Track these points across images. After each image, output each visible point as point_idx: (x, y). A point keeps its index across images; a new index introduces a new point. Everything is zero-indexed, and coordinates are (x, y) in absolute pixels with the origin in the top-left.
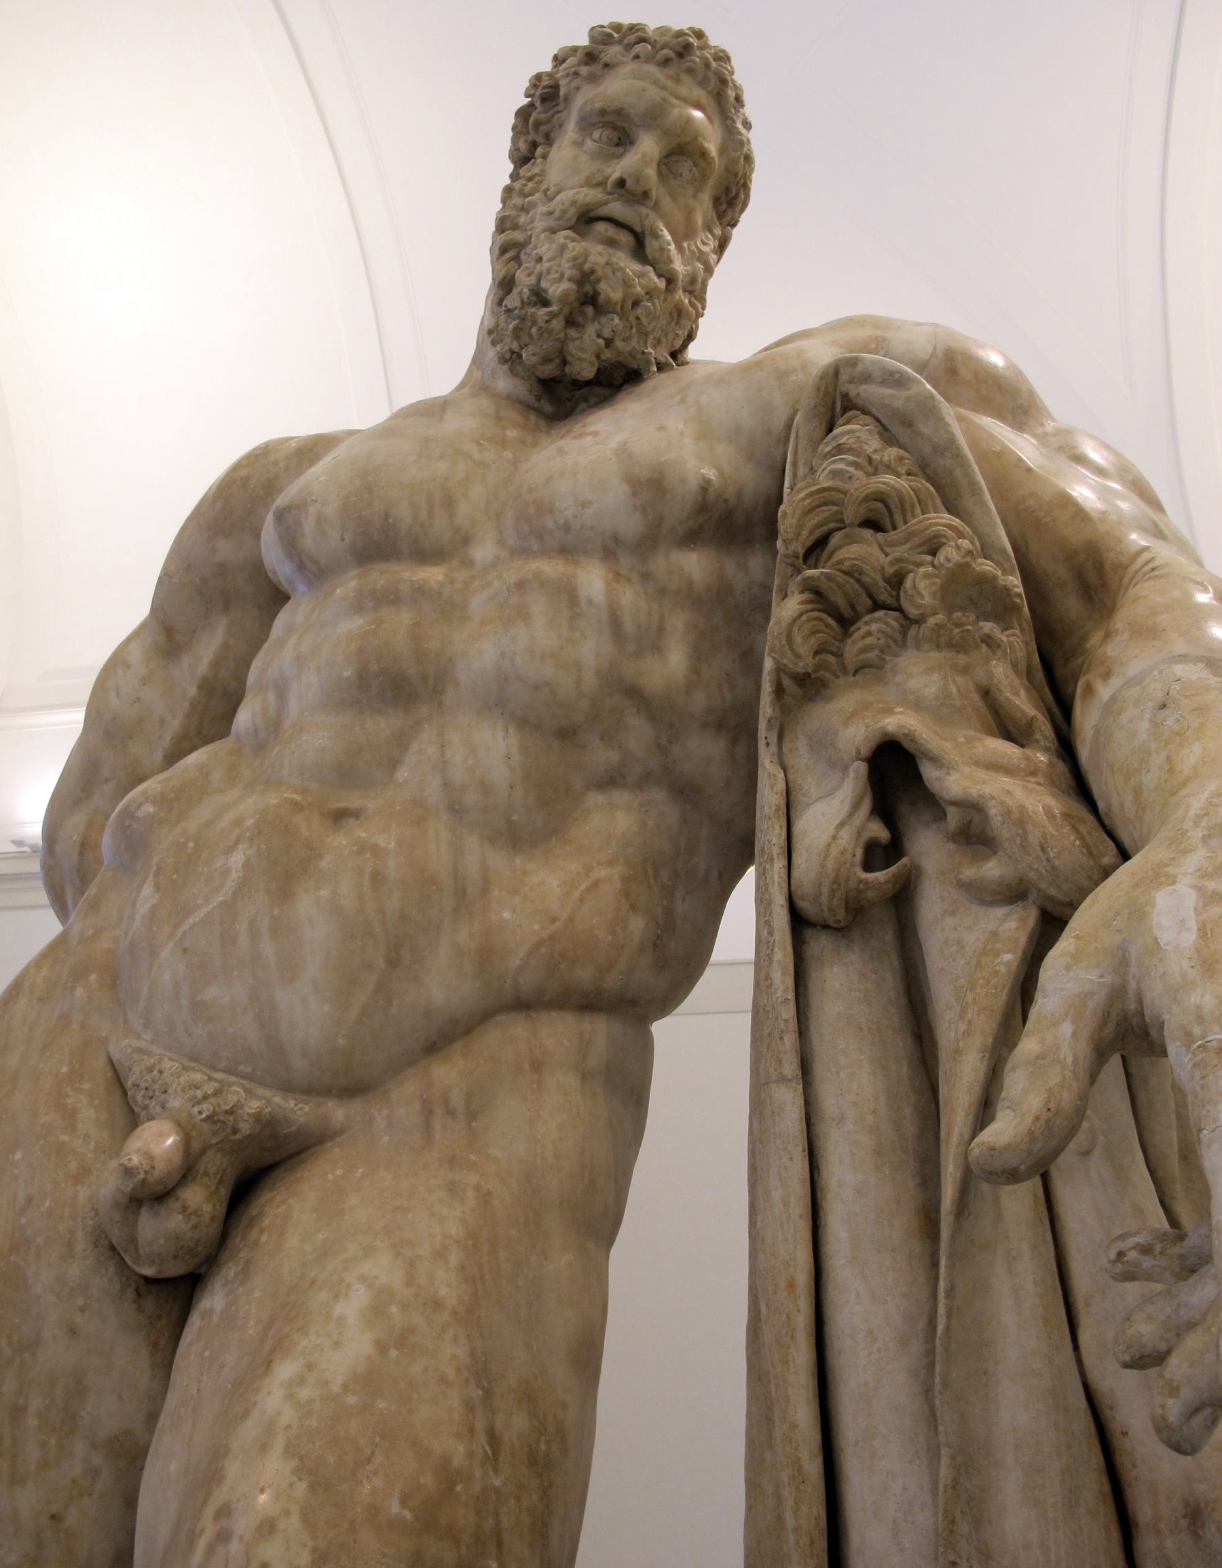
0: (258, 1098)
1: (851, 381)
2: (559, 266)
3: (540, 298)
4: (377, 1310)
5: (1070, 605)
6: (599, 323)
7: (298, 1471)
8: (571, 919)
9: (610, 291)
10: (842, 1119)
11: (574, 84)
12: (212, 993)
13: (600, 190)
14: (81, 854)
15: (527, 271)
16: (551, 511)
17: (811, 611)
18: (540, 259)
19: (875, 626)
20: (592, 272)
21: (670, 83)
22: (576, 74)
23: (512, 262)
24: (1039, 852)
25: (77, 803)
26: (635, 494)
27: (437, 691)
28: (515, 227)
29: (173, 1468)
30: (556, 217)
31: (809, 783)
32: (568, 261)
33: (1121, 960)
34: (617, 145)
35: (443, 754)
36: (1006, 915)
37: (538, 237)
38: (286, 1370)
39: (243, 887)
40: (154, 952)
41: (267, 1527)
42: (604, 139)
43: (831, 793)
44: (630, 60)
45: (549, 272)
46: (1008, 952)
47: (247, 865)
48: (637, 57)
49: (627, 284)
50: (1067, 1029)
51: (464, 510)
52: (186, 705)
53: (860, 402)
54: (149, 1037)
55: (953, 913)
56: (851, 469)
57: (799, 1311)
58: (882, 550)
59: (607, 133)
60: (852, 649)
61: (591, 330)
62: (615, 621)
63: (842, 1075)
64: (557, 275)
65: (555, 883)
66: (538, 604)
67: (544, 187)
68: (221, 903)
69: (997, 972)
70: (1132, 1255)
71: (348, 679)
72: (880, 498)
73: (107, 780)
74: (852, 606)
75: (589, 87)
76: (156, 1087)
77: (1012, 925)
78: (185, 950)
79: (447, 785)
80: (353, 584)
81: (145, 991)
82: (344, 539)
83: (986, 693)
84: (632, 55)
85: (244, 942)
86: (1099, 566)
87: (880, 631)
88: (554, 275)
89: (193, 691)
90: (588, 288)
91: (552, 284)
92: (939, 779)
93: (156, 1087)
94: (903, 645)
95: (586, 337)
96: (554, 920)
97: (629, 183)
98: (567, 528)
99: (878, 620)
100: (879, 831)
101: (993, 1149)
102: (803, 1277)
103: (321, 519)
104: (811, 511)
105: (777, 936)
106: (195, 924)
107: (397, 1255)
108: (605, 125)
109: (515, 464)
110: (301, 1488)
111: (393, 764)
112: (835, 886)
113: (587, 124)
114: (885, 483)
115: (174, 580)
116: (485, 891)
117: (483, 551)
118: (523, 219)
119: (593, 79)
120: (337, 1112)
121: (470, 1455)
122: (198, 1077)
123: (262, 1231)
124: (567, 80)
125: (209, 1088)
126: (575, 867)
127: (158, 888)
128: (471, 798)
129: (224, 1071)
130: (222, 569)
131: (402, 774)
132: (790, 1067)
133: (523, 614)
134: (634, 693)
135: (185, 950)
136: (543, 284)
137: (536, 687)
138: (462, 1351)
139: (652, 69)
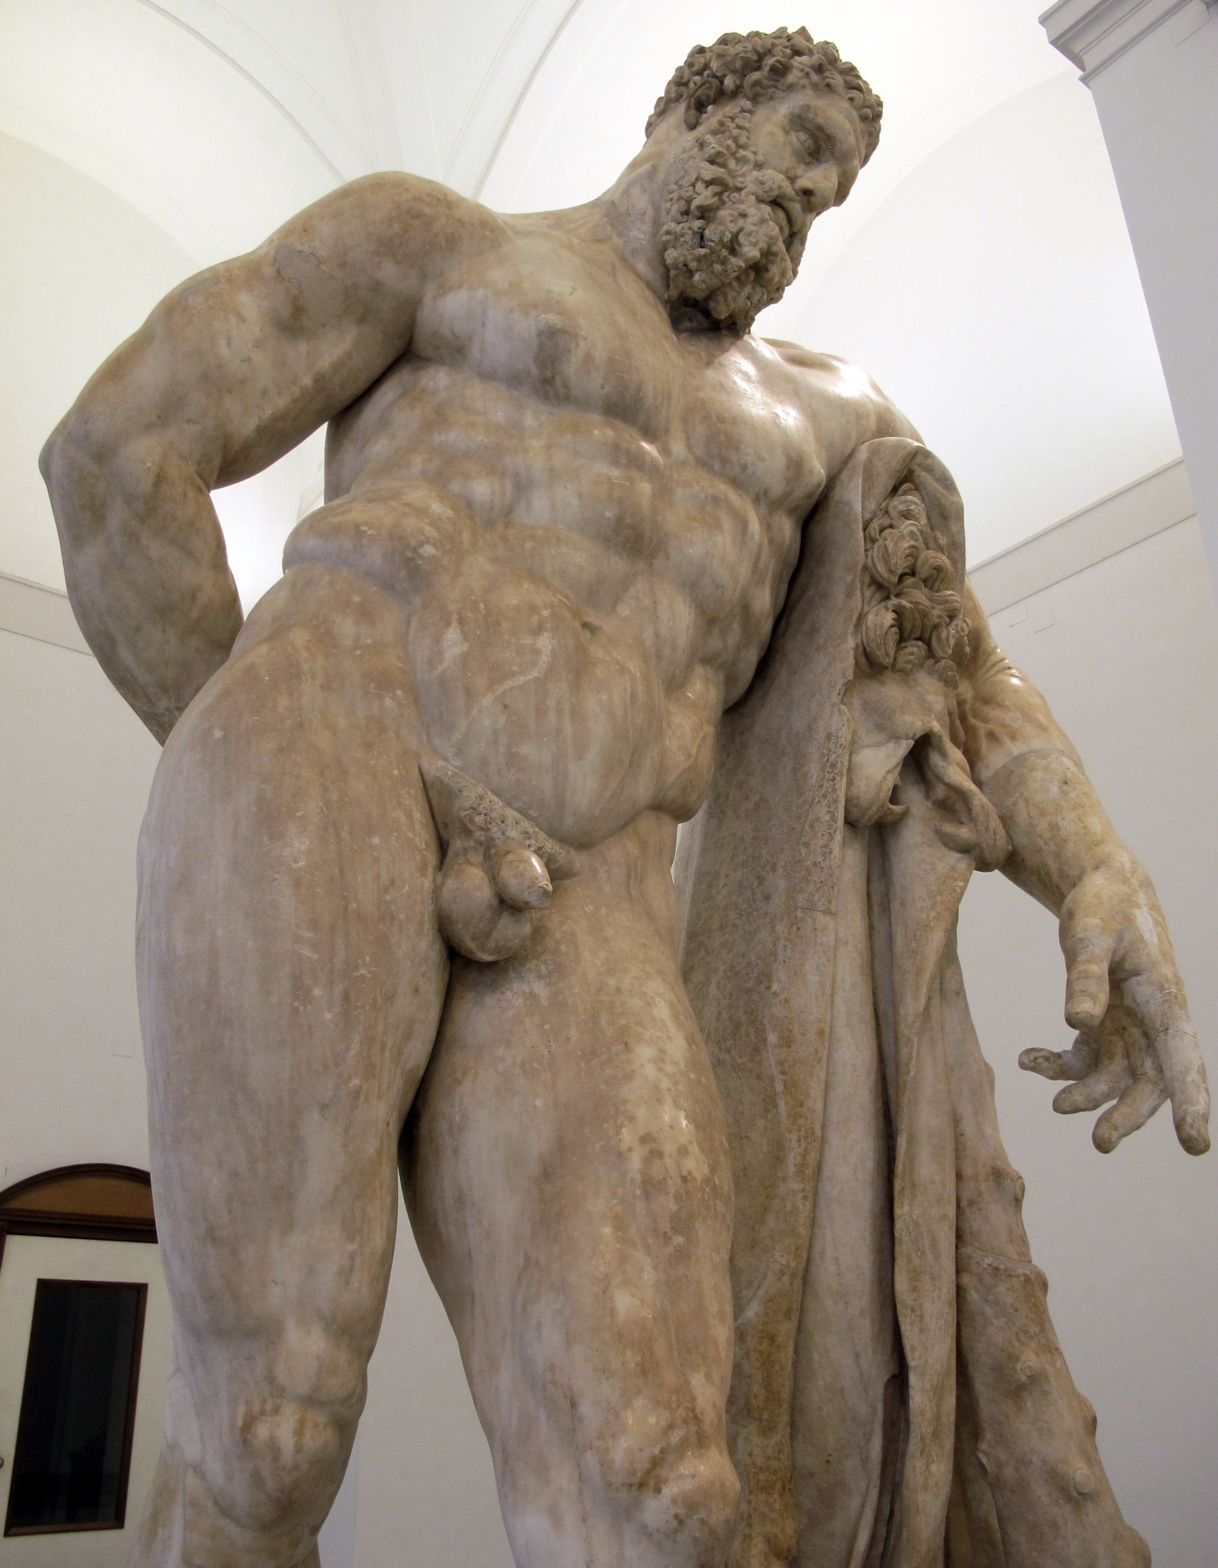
3: (733, 247)
6: (753, 288)
10: (846, 943)
12: (525, 749)
15: (731, 218)
16: (738, 449)
18: (744, 216)
19: (915, 649)
22: (807, 75)
23: (717, 197)
24: (992, 835)
25: (148, 427)
26: (788, 468)
27: (652, 556)
28: (723, 166)
30: (764, 190)
32: (765, 235)
35: (655, 609)
38: (644, 1053)
40: (470, 694)
41: (683, 1151)
42: (806, 145)
43: (877, 745)
44: (847, 97)
45: (750, 235)
46: (961, 881)
47: (553, 652)
48: (851, 99)
52: (297, 391)
53: (918, 481)
54: (458, 763)
55: (930, 846)
57: (824, 1048)
59: (810, 142)
61: (748, 290)
63: (848, 916)
64: (754, 240)
66: (727, 523)
68: (536, 678)
69: (955, 890)
70: (1040, 1060)
71: (608, 519)
73: (189, 421)
75: (809, 91)
78: (506, 706)
79: (657, 635)
82: (603, 388)
84: (850, 96)
88: (752, 239)
89: (307, 381)
91: (750, 245)
92: (943, 767)
93: (494, 814)
94: (921, 666)
95: (742, 294)
97: (813, 199)
98: (744, 468)
99: (919, 647)
101: (1092, 1016)
106: (513, 688)
108: (812, 135)
111: (617, 599)
112: (880, 808)
113: (799, 121)
115: (323, 267)
118: (732, 164)
119: (815, 87)
123: (558, 943)
124: (800, 74)
128: (667, 651)
130: (377, 287)
131: (624, 610)
133: (717, 526)
135: (506, 706)
136: (741, 238)
137: (717, 587)
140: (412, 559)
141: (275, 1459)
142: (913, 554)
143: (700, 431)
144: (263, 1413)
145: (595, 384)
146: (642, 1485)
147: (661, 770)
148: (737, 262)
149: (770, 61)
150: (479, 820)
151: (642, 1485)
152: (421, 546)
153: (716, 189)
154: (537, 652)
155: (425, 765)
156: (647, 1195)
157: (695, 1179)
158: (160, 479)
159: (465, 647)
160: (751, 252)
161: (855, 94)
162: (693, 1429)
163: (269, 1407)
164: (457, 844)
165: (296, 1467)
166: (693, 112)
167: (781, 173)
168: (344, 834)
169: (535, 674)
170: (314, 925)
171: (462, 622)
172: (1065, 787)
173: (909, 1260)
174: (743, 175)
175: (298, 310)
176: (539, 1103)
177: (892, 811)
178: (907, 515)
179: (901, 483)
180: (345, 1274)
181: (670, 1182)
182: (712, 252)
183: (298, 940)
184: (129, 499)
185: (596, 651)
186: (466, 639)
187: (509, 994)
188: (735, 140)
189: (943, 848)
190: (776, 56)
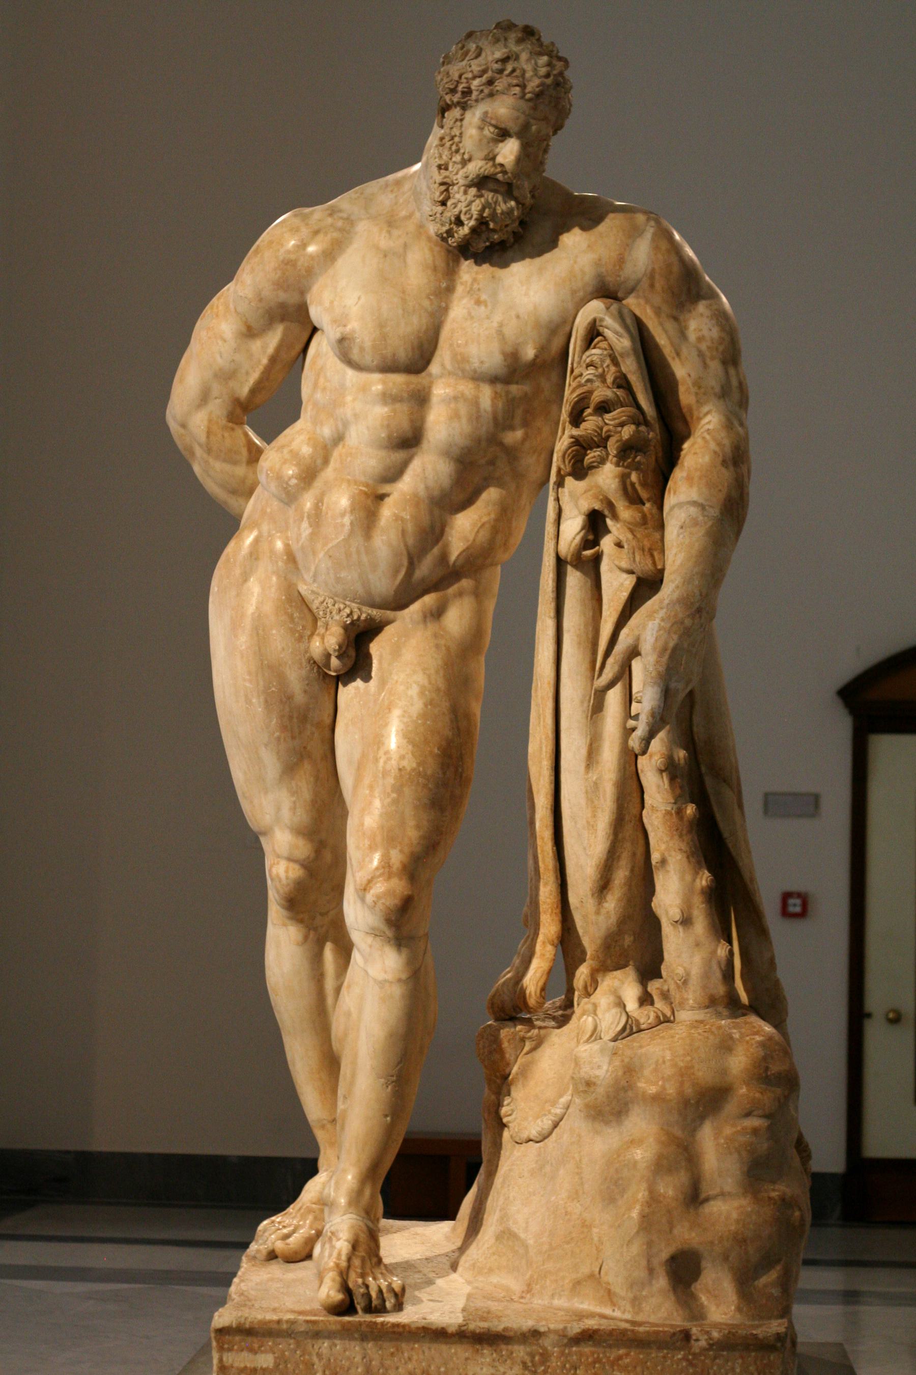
2: (470, 210)
3: (459, 222)
7: (408, 742)
8: (474, 540)
11: (481, 96)
13: (491, 163)
14: (208, 437)
16: (468, 361)
22: (482, 91)
26: (505, 360)
28: (446, 169)
29: (356, 737)
33: (638, 639)
36: (627, 578)
37: (459, 188)
39: (352, 532)
40: (314, 553)
47: (352, 523)
52: (261, 368)
61: (484, 236)
65: (468, 524)
73: (216, 398)
76: (328, 610)
78: (330, 556)
81: (313, 568)
85: (355, 556)
87: (599, 455)
89: (265, 361)
90: (484, 221)
96: (468, 541)
100: (591, 537)
106: (333, 547)
107: (424, 673)
110: (410, 747)
115: (252, 304)
119: (491, 95)
121: (453, 734)
122: (342, 606)
125: (348, 611)
126: (476, 517)
127: (310, 523)
135: (330, 556)
136: (463, 217)
140: (286, 488)
141: (280, 882)
144: (274, 864)
146: (365, 890)
148: (465, 230)
149: (460, 88)
151: (365, 890)
153: (443, 188)
154: (343, 525)
156: (383, 777)
157: (406, 770)
158: (209, 433)
162: (387, 870)
163: (276, 862)
164: (319, 623)
165: (288, 885)
168: (260, 632)
170: (250, 673)
171: (309, 517)
173: (593, 802)
176: (356, 737)
180: (293, 809)
181: (393, 771)
183: (244, 680)
184: (200, 445)
186: (311, 526)
190: (462, 83)
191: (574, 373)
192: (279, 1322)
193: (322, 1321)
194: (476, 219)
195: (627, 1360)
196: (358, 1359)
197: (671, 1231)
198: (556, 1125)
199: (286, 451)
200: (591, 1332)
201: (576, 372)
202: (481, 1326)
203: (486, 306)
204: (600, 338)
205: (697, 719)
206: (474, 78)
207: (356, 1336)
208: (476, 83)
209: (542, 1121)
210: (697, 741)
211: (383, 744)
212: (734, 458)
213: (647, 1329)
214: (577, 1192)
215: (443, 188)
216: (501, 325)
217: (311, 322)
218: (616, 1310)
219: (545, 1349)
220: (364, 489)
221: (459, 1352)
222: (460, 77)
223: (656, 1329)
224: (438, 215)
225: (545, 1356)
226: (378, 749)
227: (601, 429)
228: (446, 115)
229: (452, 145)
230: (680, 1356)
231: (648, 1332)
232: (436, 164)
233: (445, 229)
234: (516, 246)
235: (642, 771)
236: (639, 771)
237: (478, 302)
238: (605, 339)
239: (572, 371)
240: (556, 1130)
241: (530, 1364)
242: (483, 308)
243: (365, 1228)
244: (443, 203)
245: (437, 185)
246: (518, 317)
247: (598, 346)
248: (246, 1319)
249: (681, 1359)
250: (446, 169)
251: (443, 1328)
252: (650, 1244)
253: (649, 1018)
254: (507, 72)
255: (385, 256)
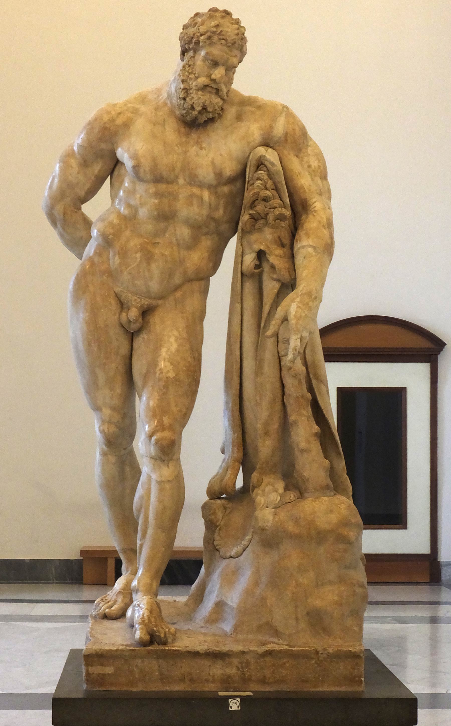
0: (147, 301)
1: (263, 159)
3: (193, 108)
4: (176, 341)
5: (300, 209)
9: (210, 109)
12: (136, 282)
17: (250, 219)
19: (261, 222)
20: (207, 105)
21: (229, 52)
22: (205, 42)
26: (215, 177)
31: (247, 250)
34: (215, 65)
38: (164, 350)
39: (140, 262)
40: (122, 272)
41: (168, 372)
43: (250, 253)
47: (140, 257)
48: (222, 44)
49: (214, 107)
50: (279, 320)
51: (177, 170)
56: (261, 185)
58: (265, 206)
60: (257, 226)
61: (204, 115)
62: (210, 205)
66: (195, 202)
67: (194, 73)
72: (265, 197)
74: (258, 218)
77: (277, 285)
78: (130, 273)
79: (177, 239)
80: (154, 190)
83: (279, 237)
84: (221, 43)
86: (306, 203)
89: (93, 178)
90: (205, 107)
96: (196, 266)
98: (201, 182)
100: (258, 263)
102: (239, 334)
103: (145, 171)
104: (253, 196)
105: (239, 279)
109: (186, 152)
110: (172, 367)
111: (164, 232)
114: (267, 194)
116: (184, 260)
117: (181, 181)
118: (188, 81)
119: (210, 45)
120: (160, 302)
125: (139, 300)
128: (181, 242)
129: (139, 295)
130: (102, 150)
131: (167, 235)
132: (239, 301)
134: (213, 218)
135: (130, 273)
136: (194, 106)
138: (189, 345)
139: (225, 48)
142: (258, 193)
143: (187, 173)
145: (148, 176)
147: (185, 273)
148: (195, 113)
149: (194, 40)
150: (125, 301)
152: (109, 236)
153: (185, 91)
154: (136, 258)
155: (115, 291)
156: (159, 382)
157: (170, 378)
159: (119, 261)
160: (198, 108)
161: (223, 41)
164: (124, 306)
166: (182, 55)
167: (204, 77)
169: (136, 264)
172: (304, 260)
174: (192, 84)
175: (85, 161)
177: (255, 272)
178: (259, 179)
179: (261, 165)
180: (112, 397)
182: (188, 111)
185: (157, 251)
186: (120, 258)
187: (140, 338)
188: (188, 72)
189: (272, 280)
190: (194, 38)
191: (250, 183)
192: (117, 650)
193: (138, 649)
194: (202, 107)
195: (287, 665)
196: (156, 667)
197: (306, 600)
198: (244, 550)
199: (106, 222)
200: (271, 651)
201: (251, 182)
202: (217, 650)
203: (205, 150)
204: (263, 166)
205: (307, 352)
206: (201, 35)
207: (155, 656)
208: (202, 38)
209: (237, 548)
210: (308, 362)
211: (158, 365)
212: (328, 224)
213: (298, 649)
214: (257, 582)
215: (185, 91)
216: (213, 159)
217: (117, 158)
218: (280, 640)
219: (247, 660)
220: (146, 240)
221: (207, 663)
222: (194, 35)
223: (302, 649)
224: (182, 105)
225: (248, 664)
226: (156, 368)
227: (264, 211)
228: (185, 54)
229: (189, 69)
230: (313, 662)
231: (297, 650)
232: (181, 79)
233: (184, 112)
234: (219, 121)
235: (284, 377)
236: (282, 376)
237: (201, 148)
238: (266, 166)
239: (248, 182)
240: (245, 552)
241: (240, 667)
242: (204, 150)
243: (155, 603)
244: (184, 99)
245: (181, 90)
246: (221, 155)
247: (262, 169)
248: (101, 649)
249: (314, 663)
250: (186, 81)
251: (198, 651)
252: (296, 607)
253: (290, 496)
254: (218, 33)
255: (154, 125)
